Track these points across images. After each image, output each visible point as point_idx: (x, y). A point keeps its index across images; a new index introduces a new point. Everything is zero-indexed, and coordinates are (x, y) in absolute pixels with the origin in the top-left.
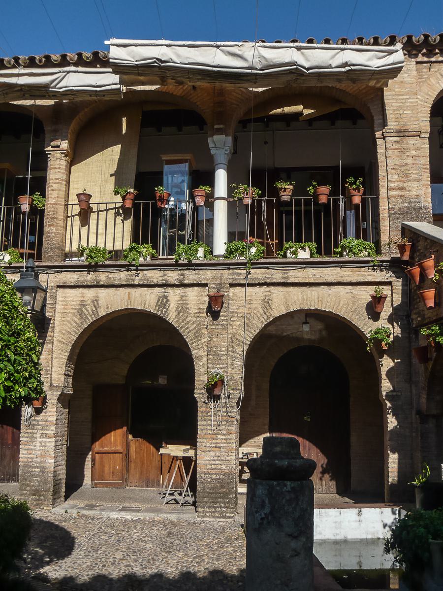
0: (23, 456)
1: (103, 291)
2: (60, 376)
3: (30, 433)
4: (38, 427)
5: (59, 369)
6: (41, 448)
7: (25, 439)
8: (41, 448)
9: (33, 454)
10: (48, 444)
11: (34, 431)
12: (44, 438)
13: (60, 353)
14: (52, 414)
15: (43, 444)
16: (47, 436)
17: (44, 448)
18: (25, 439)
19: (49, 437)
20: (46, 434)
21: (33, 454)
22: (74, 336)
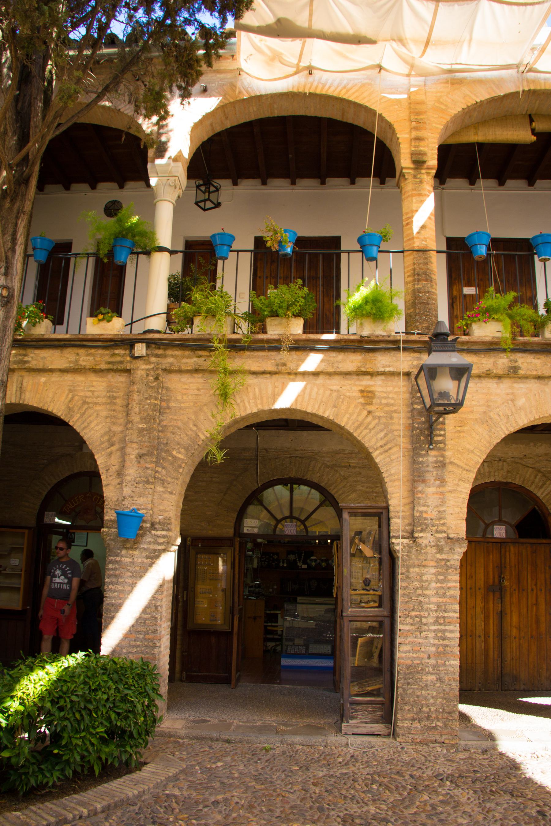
0: (404, 655)
1: (521, 385)
2: (459, 522)
3: (416, 617)
4: (428, 606)
5: (457, 510)
6: (436, 642)
7: (407, 628)
8: (436, 642)
9: (423, 652)
10: (448, 635)
11: (422, 613)
12: (440, 624)
13: (457, 485)
14: (454, 584)
15: (439, 635)
16: (446, 621)
17: (441, 642)
18: (407, 628)
19: (449, 623)
20: (444, 617)
21: (423, 652)
22: (479, 456)
